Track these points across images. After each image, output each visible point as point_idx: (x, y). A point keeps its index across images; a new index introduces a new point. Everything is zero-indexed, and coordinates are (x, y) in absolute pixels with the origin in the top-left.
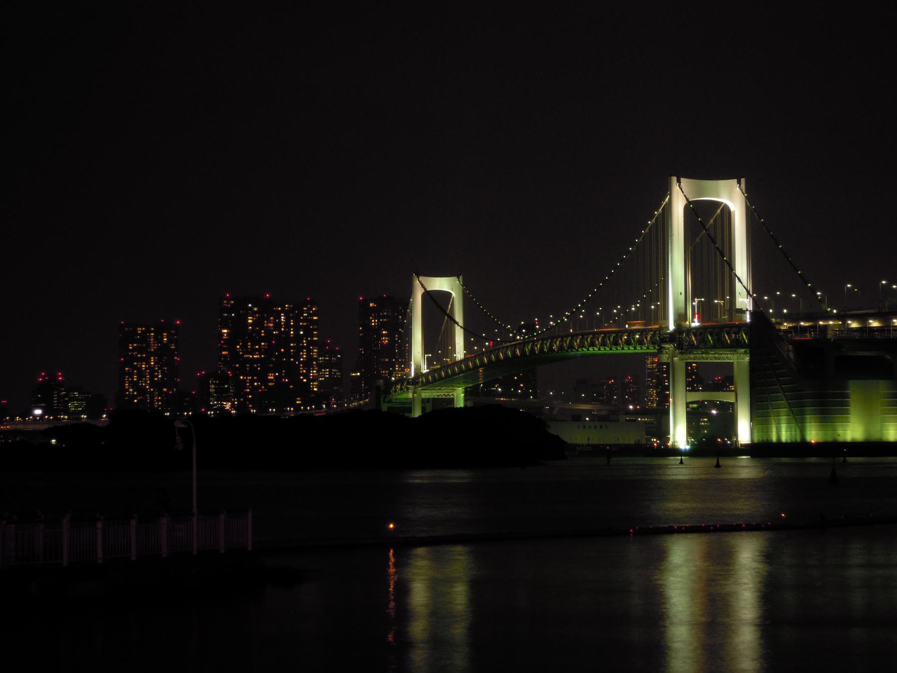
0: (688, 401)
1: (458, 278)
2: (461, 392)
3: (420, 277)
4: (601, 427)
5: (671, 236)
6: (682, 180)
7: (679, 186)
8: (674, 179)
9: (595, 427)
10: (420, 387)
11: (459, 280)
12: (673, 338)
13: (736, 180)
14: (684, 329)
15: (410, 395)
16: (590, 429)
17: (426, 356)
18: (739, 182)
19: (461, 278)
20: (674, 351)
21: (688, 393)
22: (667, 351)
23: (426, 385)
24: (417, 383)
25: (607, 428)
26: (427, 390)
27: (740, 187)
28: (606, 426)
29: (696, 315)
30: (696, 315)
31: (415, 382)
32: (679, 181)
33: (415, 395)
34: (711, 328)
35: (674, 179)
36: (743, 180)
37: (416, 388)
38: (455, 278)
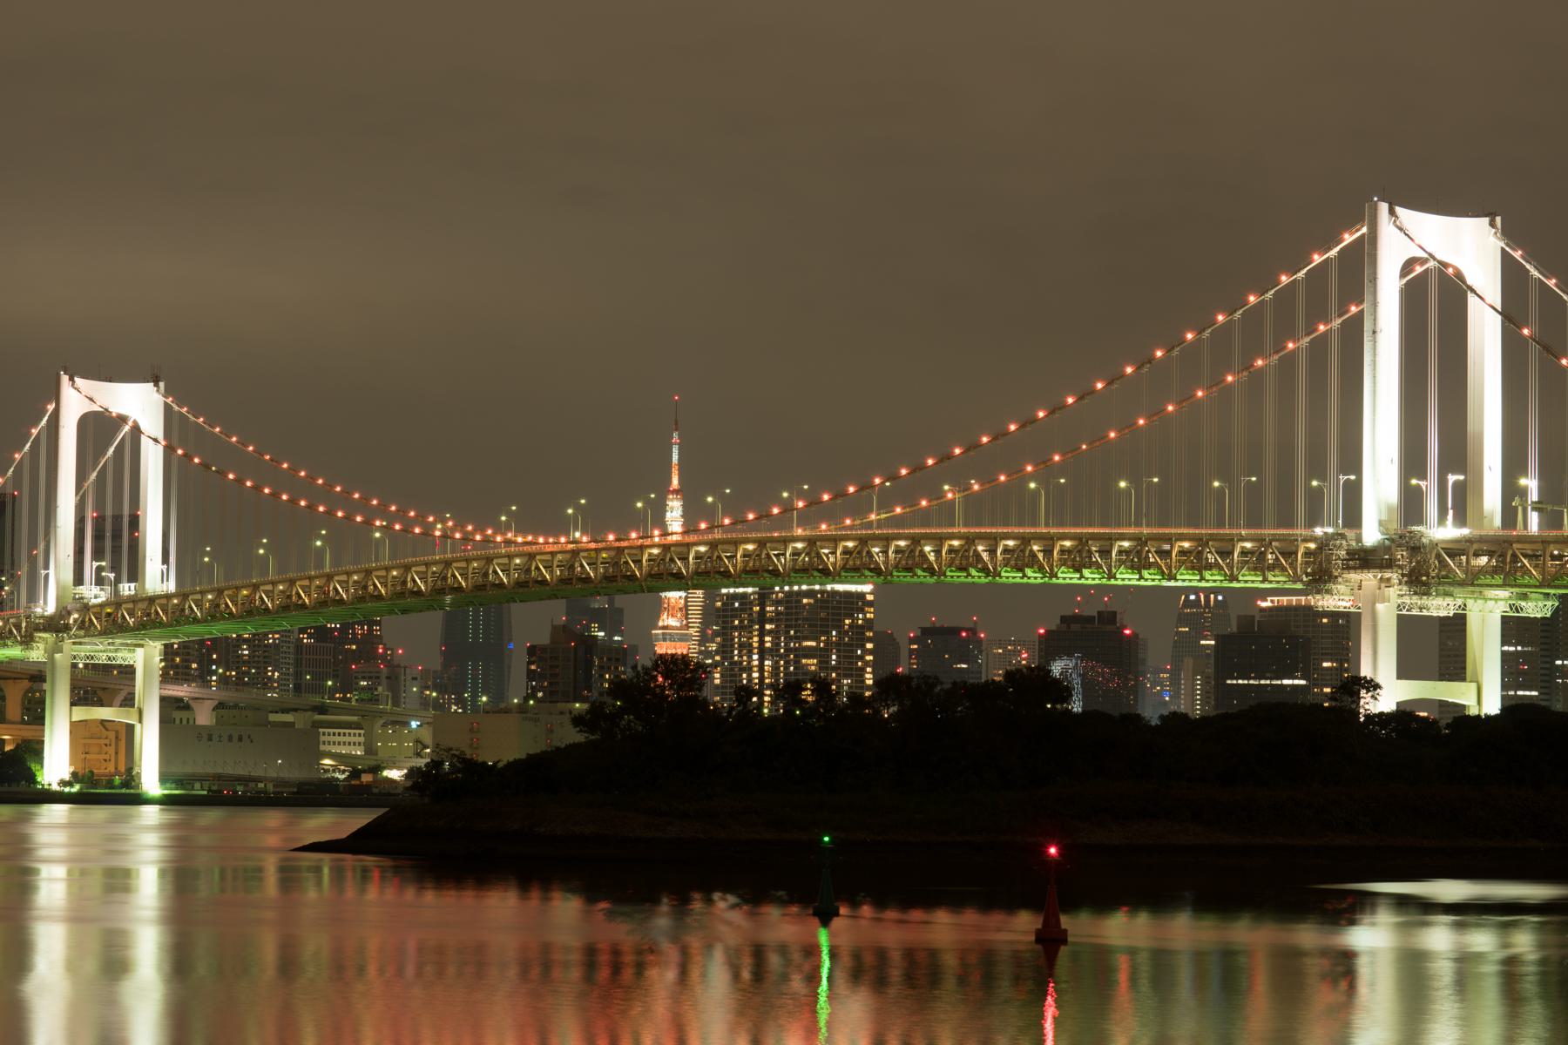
0: (1398, 701)
1: (156, 385)
2: (157, 652)
3: (76, 379)
4: (240, 739)
5: (1374, 332)
6: (1399, 210)
7: (1395, 221)
8: (1384, 207)
9: (230, 738)
10: (70, 638)
11: (158, 391)
12: (1365, 559)
13: (1486, 220)
14: (1424, 540)
15: (37, 654)
16: (220, 741)
17: (96, 564)
18: (1492, 224)
19: (162, 384)
20: (1380, 588)
21: (1399, 681)
22: (1339, 587)
23: (105, 633)
24: (67, 628)
25: (252, 741)
26: (85, 643)
27: (1496, 233)
28: (249, 737)
29: (1451, 512)
30: (1451, 512)
31: (55, 625)
32: (1392, 212)
33: (57, 656)
34: (1479, 541)
35: (1384, 207)
36: (1498, 219)
37: (63, 641)
38: (149, 387)
